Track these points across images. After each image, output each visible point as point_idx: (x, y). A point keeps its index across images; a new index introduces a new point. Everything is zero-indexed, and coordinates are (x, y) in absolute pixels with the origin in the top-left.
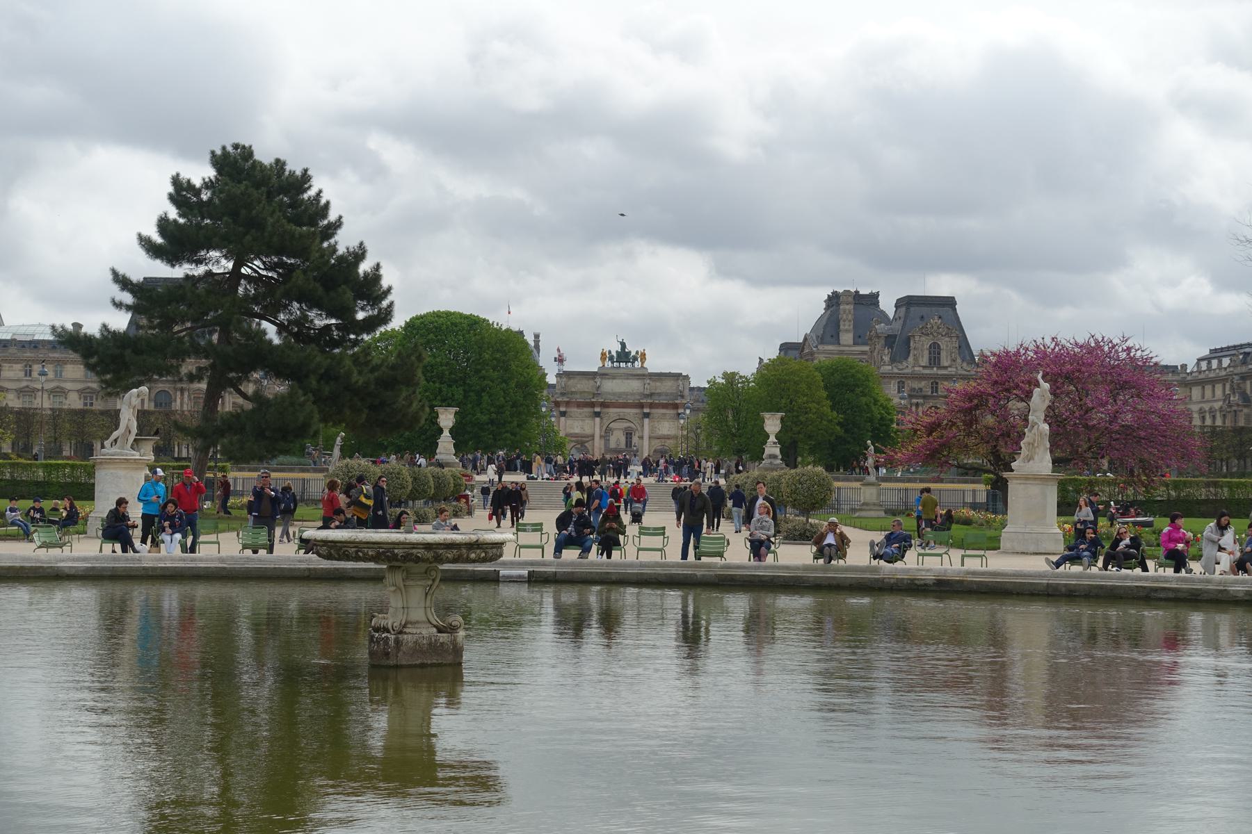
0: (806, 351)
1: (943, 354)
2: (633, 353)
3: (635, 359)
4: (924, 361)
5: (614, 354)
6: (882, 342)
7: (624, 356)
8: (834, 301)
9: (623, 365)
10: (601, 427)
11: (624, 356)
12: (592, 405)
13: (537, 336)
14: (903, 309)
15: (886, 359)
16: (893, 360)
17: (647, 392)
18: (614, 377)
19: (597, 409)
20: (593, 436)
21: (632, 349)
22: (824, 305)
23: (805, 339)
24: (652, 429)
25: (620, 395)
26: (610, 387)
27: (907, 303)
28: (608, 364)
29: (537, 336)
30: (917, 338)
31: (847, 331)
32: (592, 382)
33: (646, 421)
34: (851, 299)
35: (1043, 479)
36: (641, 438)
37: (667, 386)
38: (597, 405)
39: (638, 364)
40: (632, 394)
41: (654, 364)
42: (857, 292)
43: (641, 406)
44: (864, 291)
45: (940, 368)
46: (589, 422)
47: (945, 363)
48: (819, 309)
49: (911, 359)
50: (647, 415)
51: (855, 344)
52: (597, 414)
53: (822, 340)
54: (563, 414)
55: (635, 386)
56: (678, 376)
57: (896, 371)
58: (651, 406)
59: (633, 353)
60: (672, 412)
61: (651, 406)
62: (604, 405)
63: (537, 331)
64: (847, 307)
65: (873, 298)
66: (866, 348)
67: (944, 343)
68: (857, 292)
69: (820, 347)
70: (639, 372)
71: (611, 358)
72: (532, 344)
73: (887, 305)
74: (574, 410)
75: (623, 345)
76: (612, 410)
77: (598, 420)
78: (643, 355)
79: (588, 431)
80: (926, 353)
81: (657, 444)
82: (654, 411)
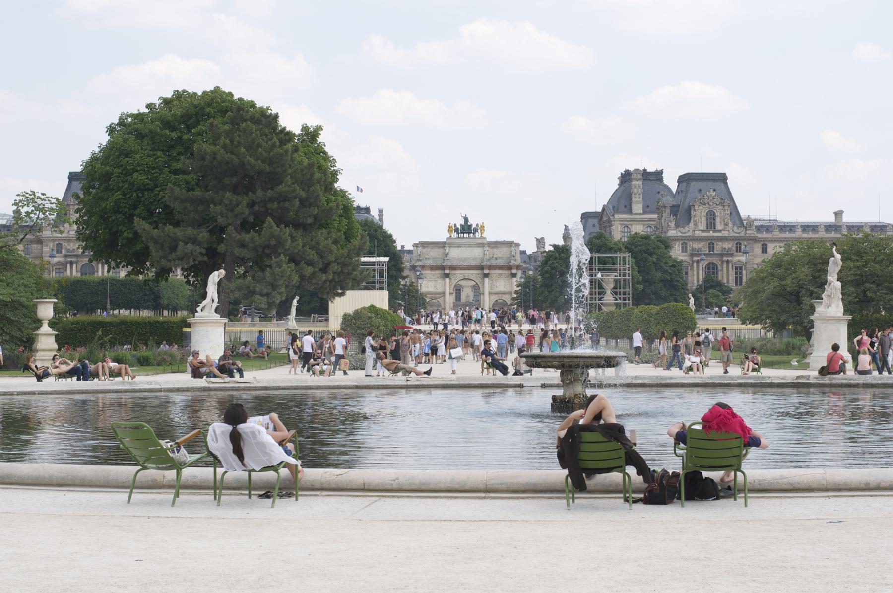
0: (605, 219)
1: (718, 220)
2: (474, 226)
3: (476, 230)
4: (702, 225)
5: (459, 226)
6: (668, 211)
7: (467, 228)
8: (626, 177)
9: (466, 235)
10: (450, 286)
11: (467, 228)
12: (443, 268)
13: (381, 211)
14: (684, 184)
15: (672, 224)
16: (677, 226)
17: (487, 257)
18: (459, 246)
19: (447, 272)
20: (444, 293)
21: (473, 222)
22: (618, 182)
23: (604, 209)
24: (491, 288)
25: (465, 259)
26: (456, 254)
27: (684, 179)
28: (455, 235)
29: (381, 211)
30: (696, 208)
31: (638, 203)
32: (441, 250)
33: (487, 280)
34: (640, 176)
35: (838, 320)
37: (502, 252)
38: (444, 270)
40: (474, 259)
41: (490, 236)
42: (645, 170)
43: (482, 268)
44: (651, 169)
45: (715, 231)
46: (440, 281)
47: (719, 227)
48: (614, 185)
49: (691, 225)
50: (486, 276)
51: (645, 213)
53: (616, 210)
55: (477, 252)
56: (510, 244)
57: (680, 234)
58: (491, 268)
59: (474, 226)
60: (506, 272)
61: (491, 268)
62: (452, 268)
63: (381, 207)
64: (637, 183)
65: (659, 175)
66: (655, 216)
67: (718, 211)
68: (645, 170)
69: (617, 216)
70: (480, 241)
71: (457, 230)
72: (377, 218)
73: (671, 181)
74: (427, 272)
75: (466, 219)
77: (447, 280)
78: (482, 227)
80: (704, 219)
81: (495, 298)
82: (492, 272)
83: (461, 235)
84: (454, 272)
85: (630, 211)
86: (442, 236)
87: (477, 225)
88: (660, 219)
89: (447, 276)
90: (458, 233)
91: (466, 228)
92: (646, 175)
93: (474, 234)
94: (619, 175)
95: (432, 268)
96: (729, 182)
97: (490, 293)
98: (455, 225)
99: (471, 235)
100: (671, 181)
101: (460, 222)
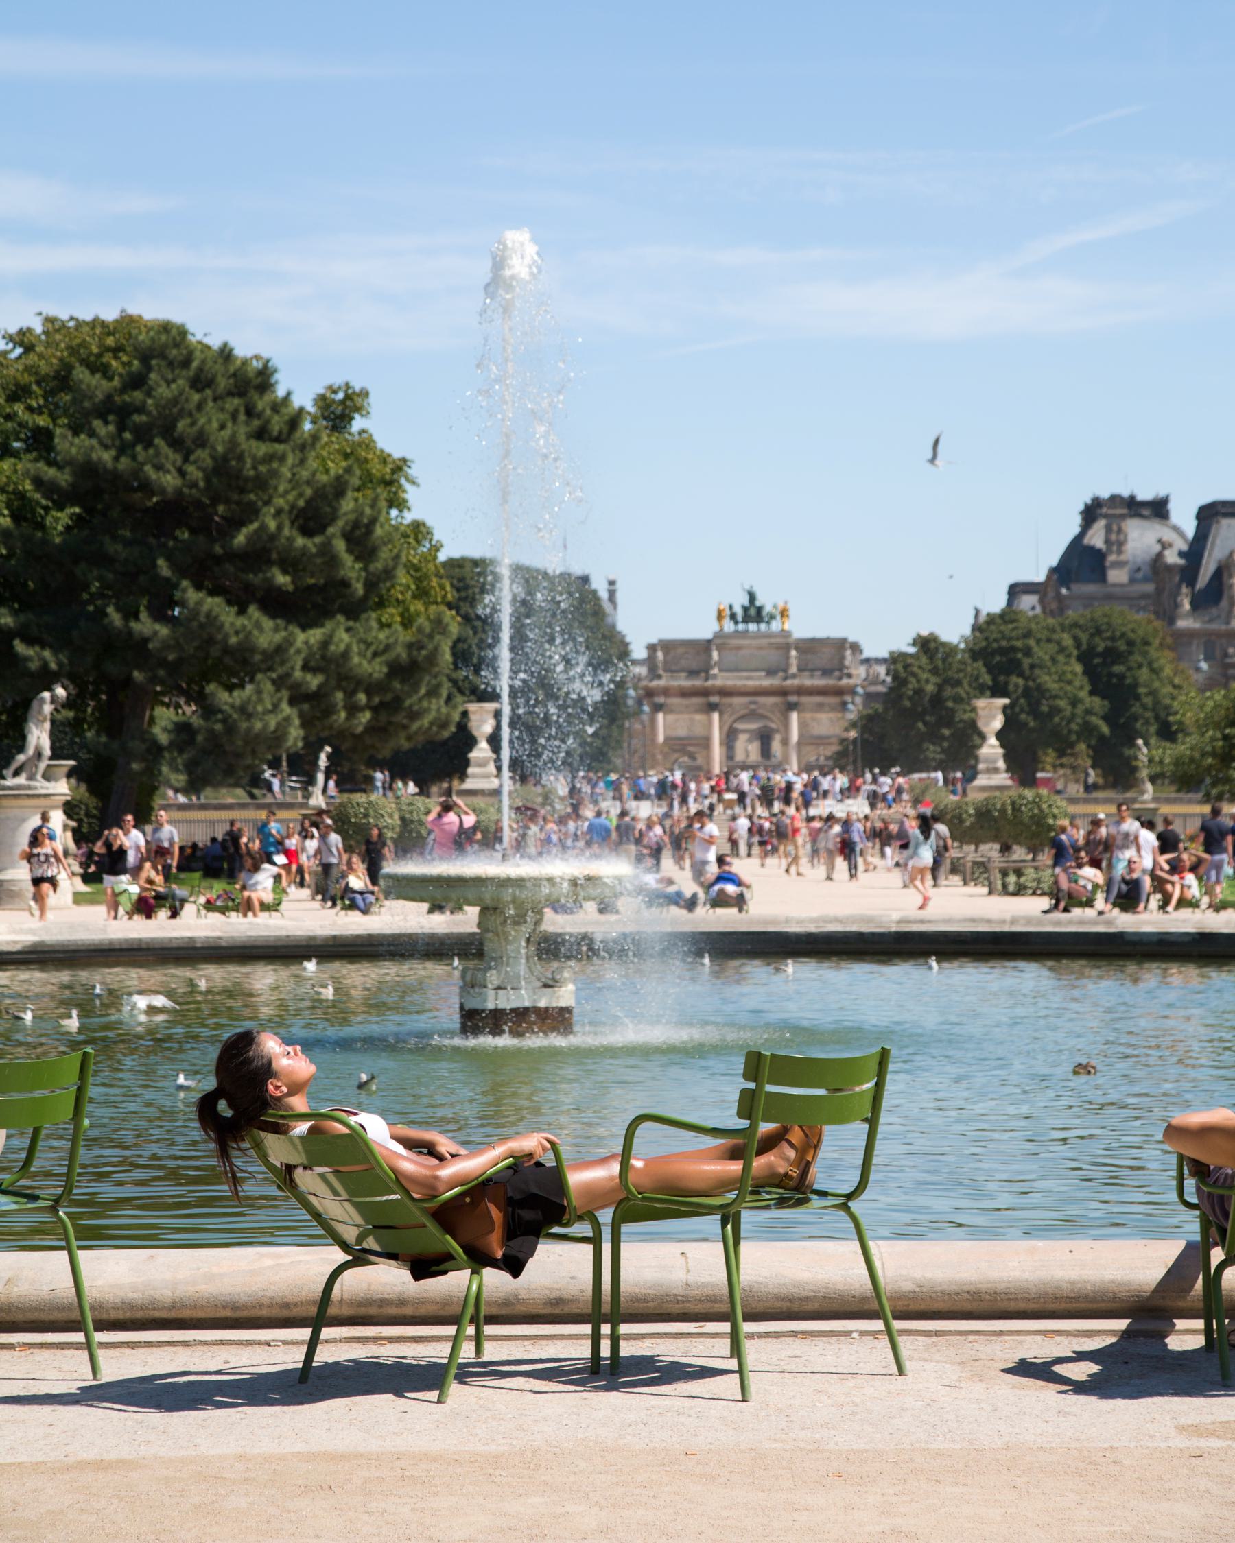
3: (772, 617)
7: (754, 612)
9: (752, 627)
21: (766, 601)
28: (729, 626)
36: (785, 742)
39: (775, 626)
41: (801, 627)
42: (1132, 498)
44: (1144, 495)
46: (699, 717)
49: (1224, 603)
50: (791, 707)
59: (768, 608)
65: (1158, 509)
68: (1132, 498)
71: (733, 617)
74: (675, 701)
75: (752, 597)
76: (737, 701)
79: (699, 731)
82: (805, 700)
83: (741, 627)
84: (727, 700)
86: (704, 629)
87: (775, 607)
88: (1159, 591)
89: (712, 707)
90: (736, 623)
91: (752, 612)
92: (1133, 507)
93: (768, 623)
94: (1082, 507)
98: (731, 607)
99: (763, 626)
101: (739, 601)
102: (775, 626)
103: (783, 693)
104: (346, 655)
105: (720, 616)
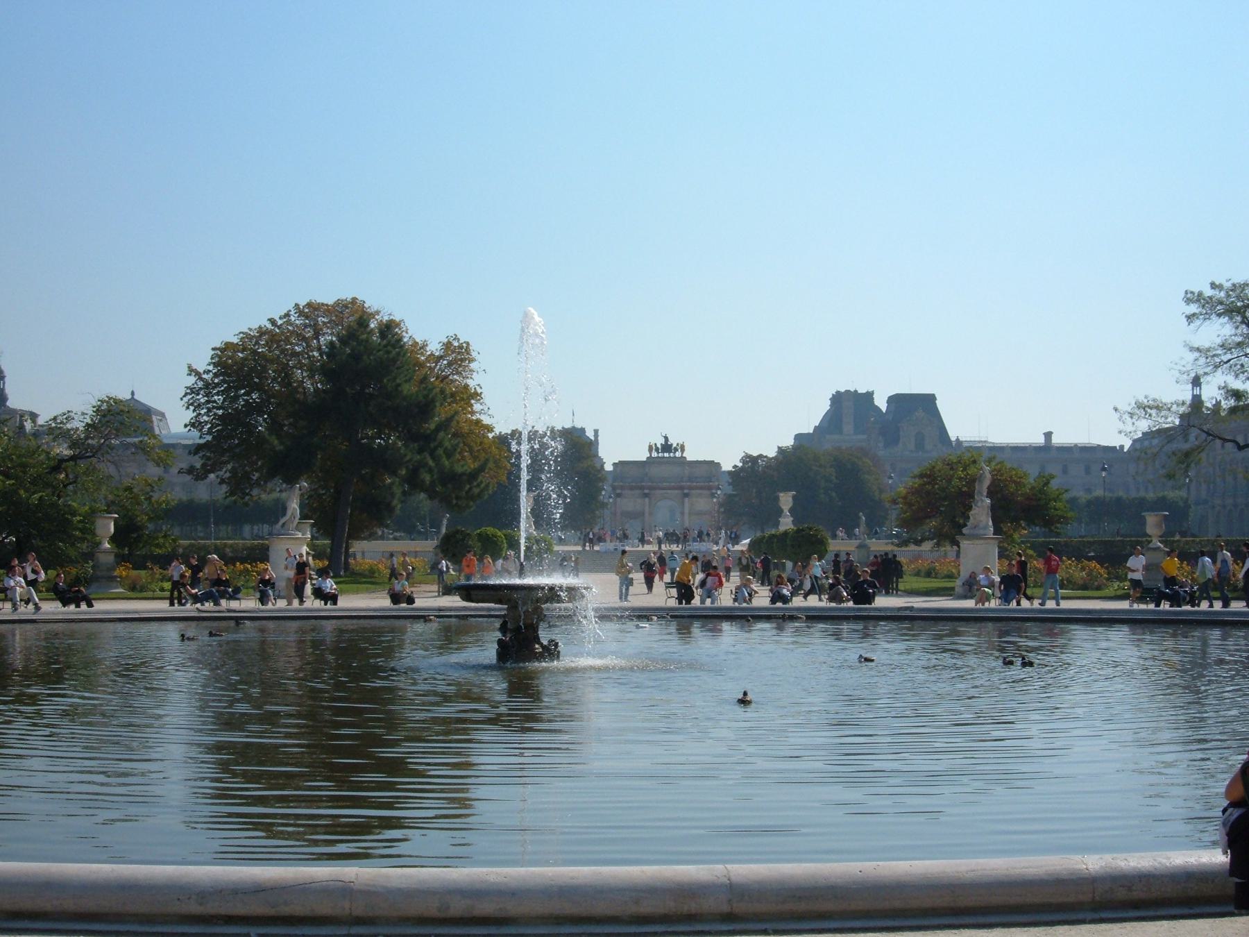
3: (676, 450)
7: (667, 447)
8: (839, 399)
9: (666, 455)
11: (667, 447)
12: (642, 488)
13: (596, 432)
15: (881, 445)
21: (673, 441)
22: (829, 402)
26: (654, 471)
27: (895, 400)
29: (596, 432)
39: (678, 454)
41: (690, 455)
44: (862, 390)
48: (826, 406)
50: (686, 495)
52: (646, 495)
54: (619, 495)
61: (691, 488)
65: (869, 396)
66: (864, 437)
69: (828, 437)
71: (657, 450)
73: (881, 403)
74: (626, 492)
75: (666, 438)
77: (647, 500)
85: (841, 432)
86: (642, 456)
95: (632, 488)
96: (940, 404)
97: (690, 514)
100: (881, 403)
101: (660, 442)
102: (678, 454)
103: (681, 488)
104: (78, 606)
105: (650, 449)
